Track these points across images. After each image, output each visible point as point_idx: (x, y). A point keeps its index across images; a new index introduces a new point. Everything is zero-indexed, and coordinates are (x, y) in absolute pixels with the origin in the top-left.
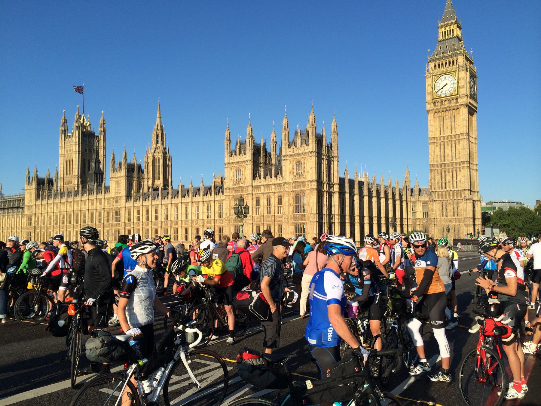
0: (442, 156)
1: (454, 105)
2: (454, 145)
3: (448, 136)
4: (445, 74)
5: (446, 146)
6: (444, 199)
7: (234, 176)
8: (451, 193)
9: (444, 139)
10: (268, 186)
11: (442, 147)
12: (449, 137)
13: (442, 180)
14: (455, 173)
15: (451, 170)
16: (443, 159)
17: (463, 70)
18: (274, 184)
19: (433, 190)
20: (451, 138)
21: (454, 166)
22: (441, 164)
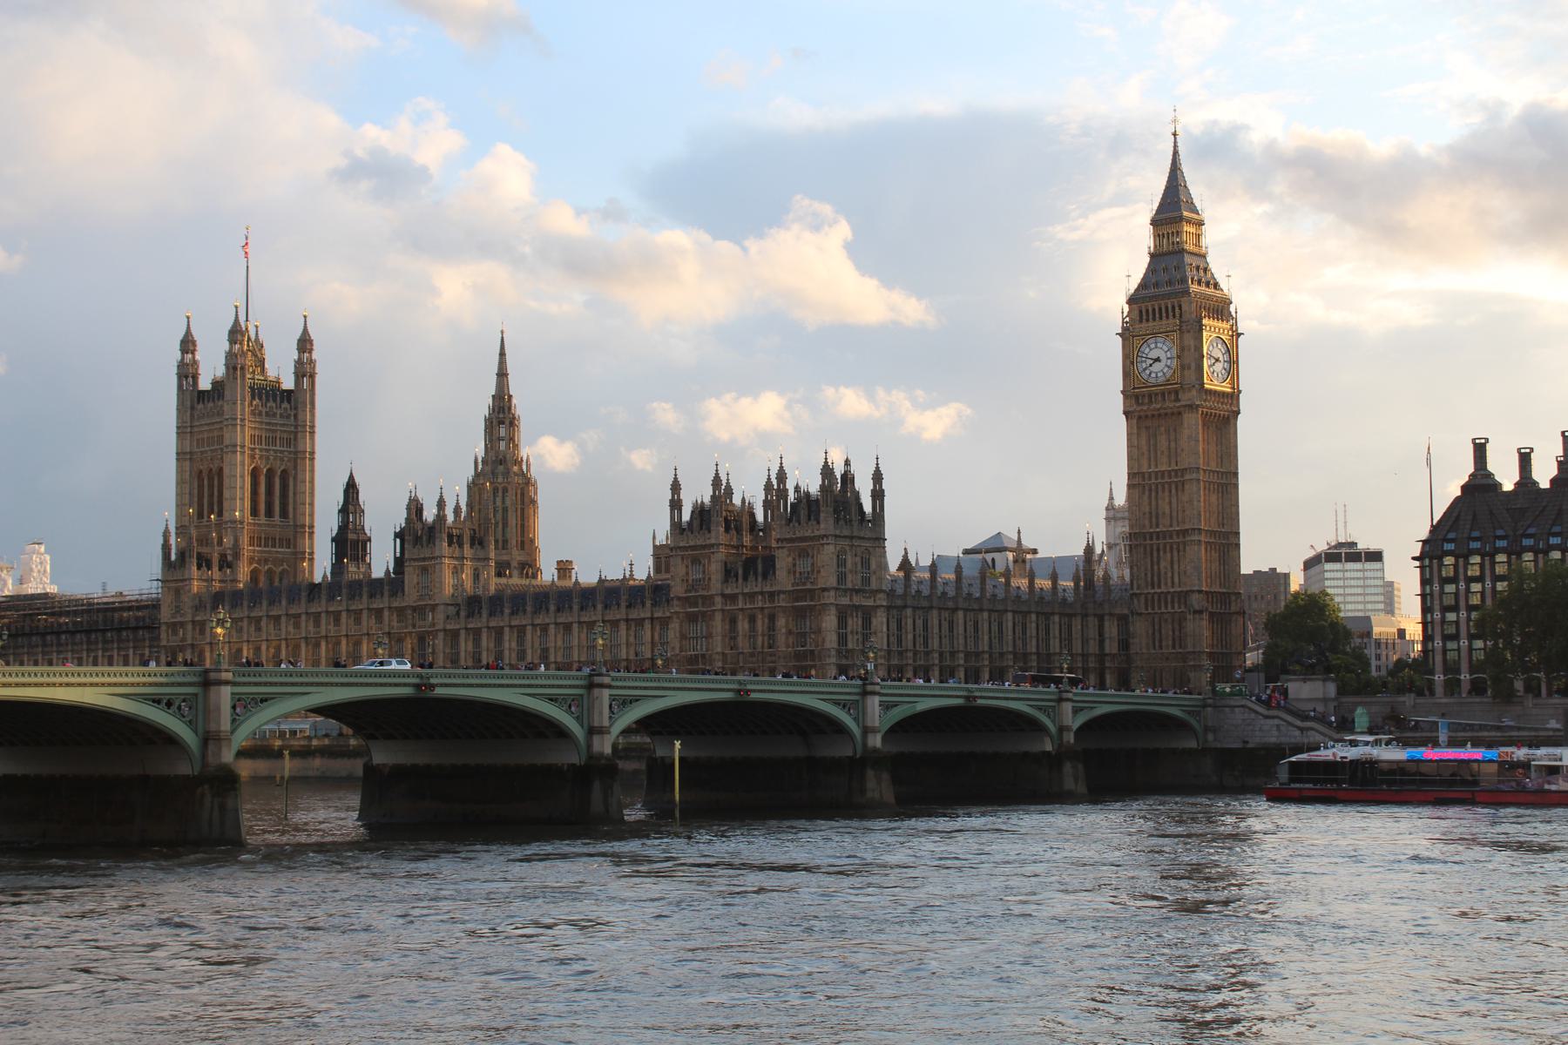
0: (1154, 514)
1: (1171, 405)
2: (1173, 491)
3: (1163, 473)
4: (1154, 334)
5: (1160, 493)
6: (1156, 610)
7: (687, 574)
8: (1169, 597)
9: (1156, 479)
10: (751, 596)
11: (1153, 494)
12: (1166, 474)
13: (1152, 569)
14: (1175, 553)
15: (1168, 548)
16: (1154, 520)
17: (1189, 332)
18: (762, 593)
19: (1136, 591)
20: (1170, 477)
21: (1175, 537)
22: (1151, 533)
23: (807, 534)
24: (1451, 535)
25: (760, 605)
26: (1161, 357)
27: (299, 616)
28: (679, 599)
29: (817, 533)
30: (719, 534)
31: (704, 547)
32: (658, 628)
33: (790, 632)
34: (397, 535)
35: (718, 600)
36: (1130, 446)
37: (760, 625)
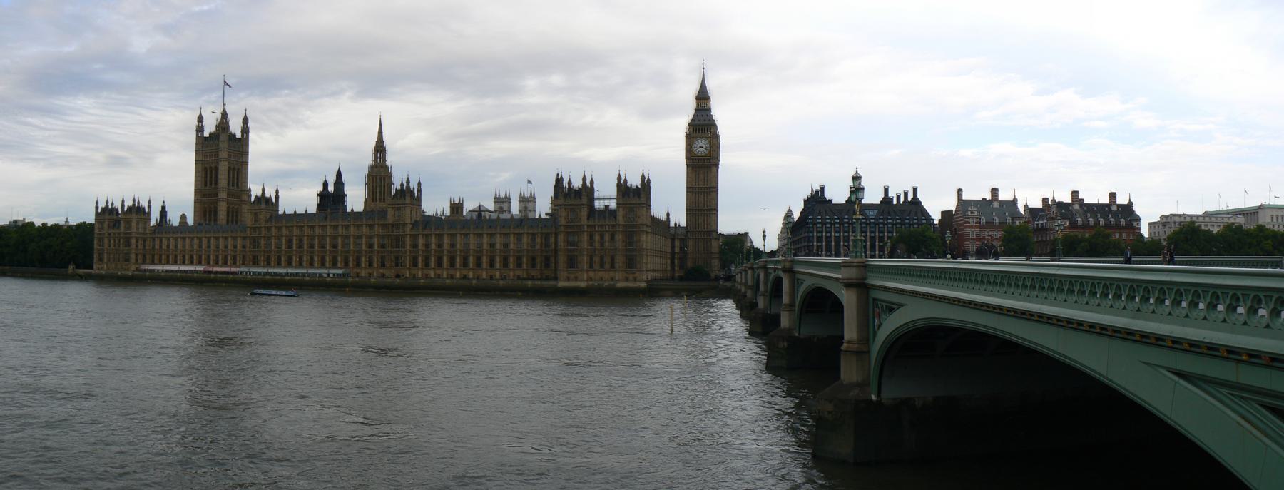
4: (701, 137)
10: (602, 226)
18: (608, 225)
21: (706, 212)
23: (632, 202)
24: (819, 217)
25: (607, 229)
26: (702, 146)
27: (326, 226)
28: (564, 226)
29: (640, 202)
30: (584, 201)
31: (579, 205)
32: (530, 237)
33: (623, 241)
34: (318, 195)
35: (586, 227)
36: (687, 177)
37: (607, 237)
